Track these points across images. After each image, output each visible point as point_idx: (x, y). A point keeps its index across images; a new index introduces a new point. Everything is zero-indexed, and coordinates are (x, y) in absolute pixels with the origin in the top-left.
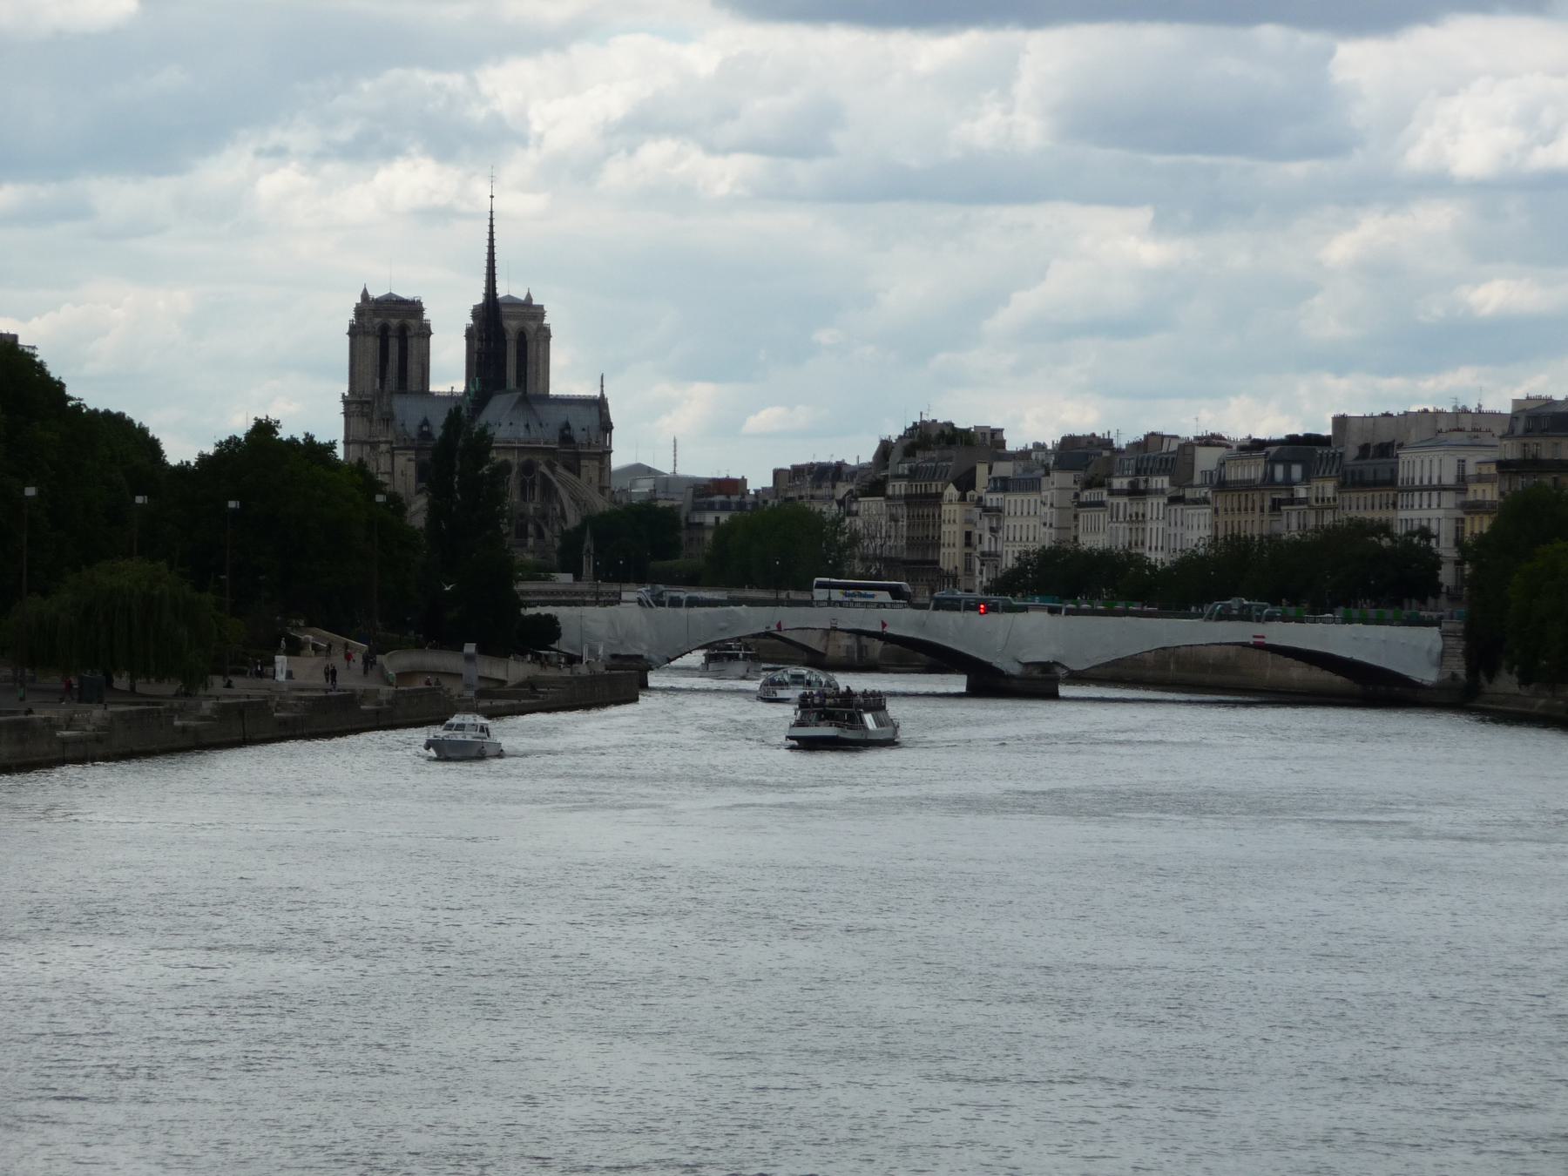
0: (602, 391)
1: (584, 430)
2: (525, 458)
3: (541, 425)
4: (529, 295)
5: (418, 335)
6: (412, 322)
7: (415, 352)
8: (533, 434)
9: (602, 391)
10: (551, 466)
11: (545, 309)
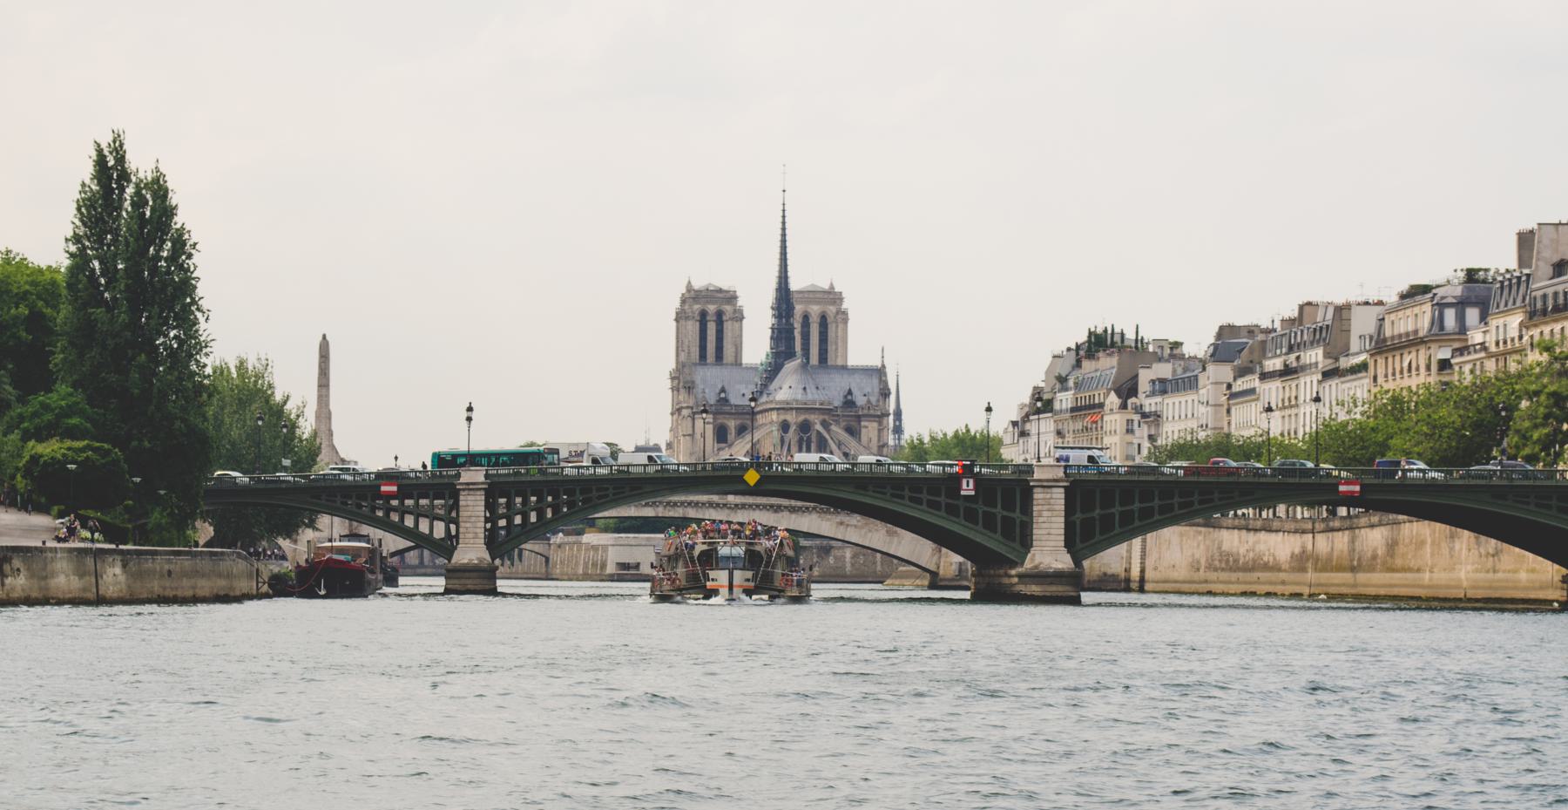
0: (883, 361)
1: (865, 395)
2: (801, 418)
3: (817, 388)
4: (832, 284)
5: (732, 319)
6: (728, 308)
7: (729, 334)
8: (810, 397)
9: (883, 361)
10: (825, 424)
11: (844, 295)
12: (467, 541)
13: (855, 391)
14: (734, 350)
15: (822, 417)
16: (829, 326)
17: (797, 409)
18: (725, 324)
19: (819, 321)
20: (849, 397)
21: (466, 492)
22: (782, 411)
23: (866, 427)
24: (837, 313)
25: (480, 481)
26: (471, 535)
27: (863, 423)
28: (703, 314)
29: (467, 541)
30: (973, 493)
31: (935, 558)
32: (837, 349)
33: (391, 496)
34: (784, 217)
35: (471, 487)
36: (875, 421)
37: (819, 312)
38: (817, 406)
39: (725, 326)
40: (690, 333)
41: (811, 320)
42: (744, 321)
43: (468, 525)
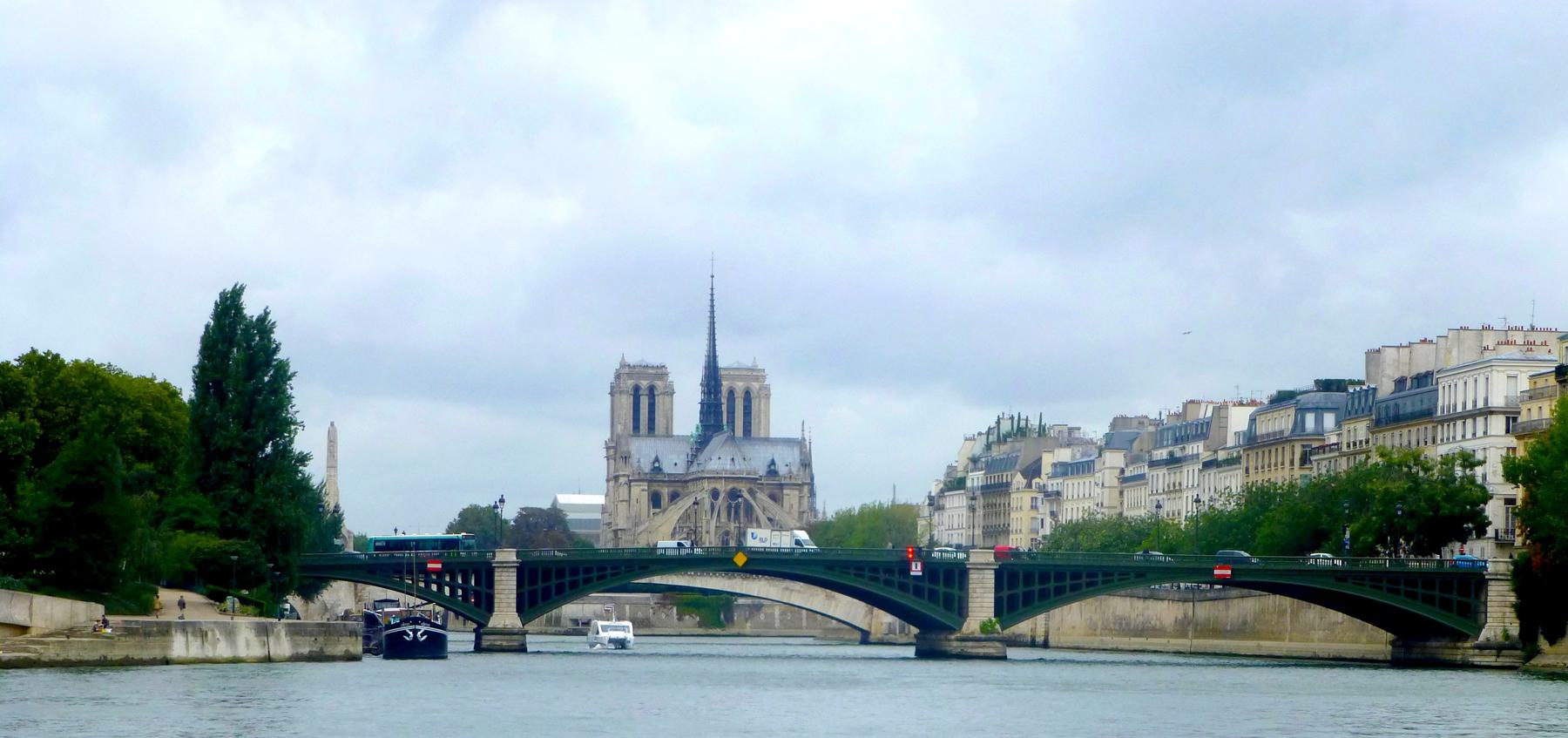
3: (744, 459)
4: (754, 362)
5: (663, 394)
6: (659, 383)
7: (661, 407)
8: (738, 467)
9: (803, 434)
10: (751, 492)
12: (502, 609)
14: (665, 421)
15: (749, 486)
16: (753, 401)
18: (656, 397)
19: (743, 396)
20: (772, 467)
21: (500, 570)
22: (712, 480)
23: (788, 495)
24: (760, 389)
25: (511, 560)
26: (504, 605)
27: (785, 491)
28: (637, 389)
29: (502, 609)
30: (920, 574)
32: (760, 422)
33: (435, 571)
34: (712, 300)
35: (504, 565)
37: (742, 389)
38: (744, 476)
39: (656, 401)
40: (625, 406)
41: (736, 395)
43: (502, 596)
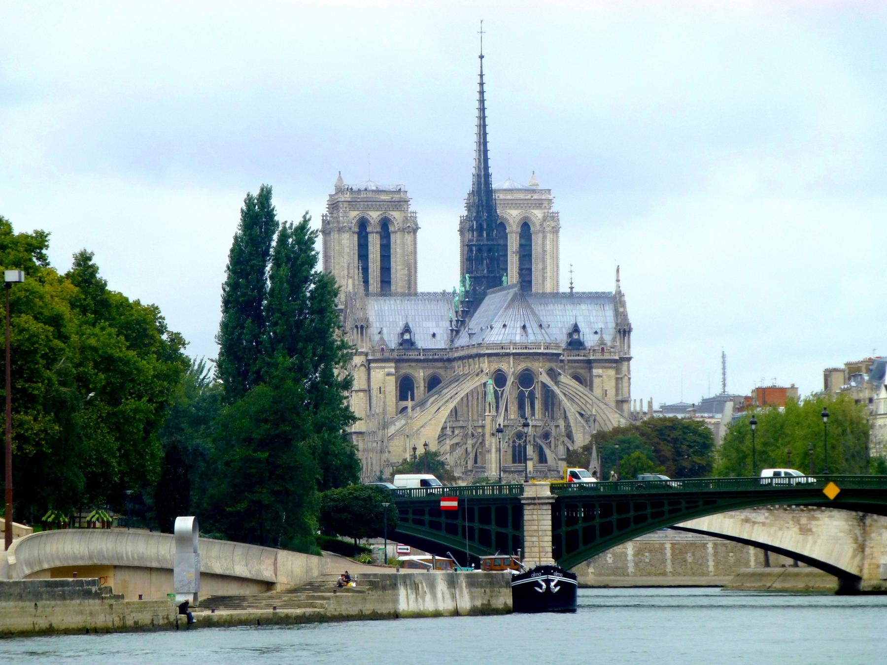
1: (596, 333)
2: (521, 367)
5: (403, 230)
6: (396, 215)
8: (531, 338)
10: (552, 373)
13: (582, 326)
15: (548, 365)
17: (514, 354)
18: (392, 237)
19: (519, 230)
20: (575, 336)
23: (600, 376)
24: (545, 219)
28: (363, 224)
31: (857, 560)
32: (544, 268)
36: (611, 368)
38: (542, 350)
42: (419, 233)
43: (535, 539)
